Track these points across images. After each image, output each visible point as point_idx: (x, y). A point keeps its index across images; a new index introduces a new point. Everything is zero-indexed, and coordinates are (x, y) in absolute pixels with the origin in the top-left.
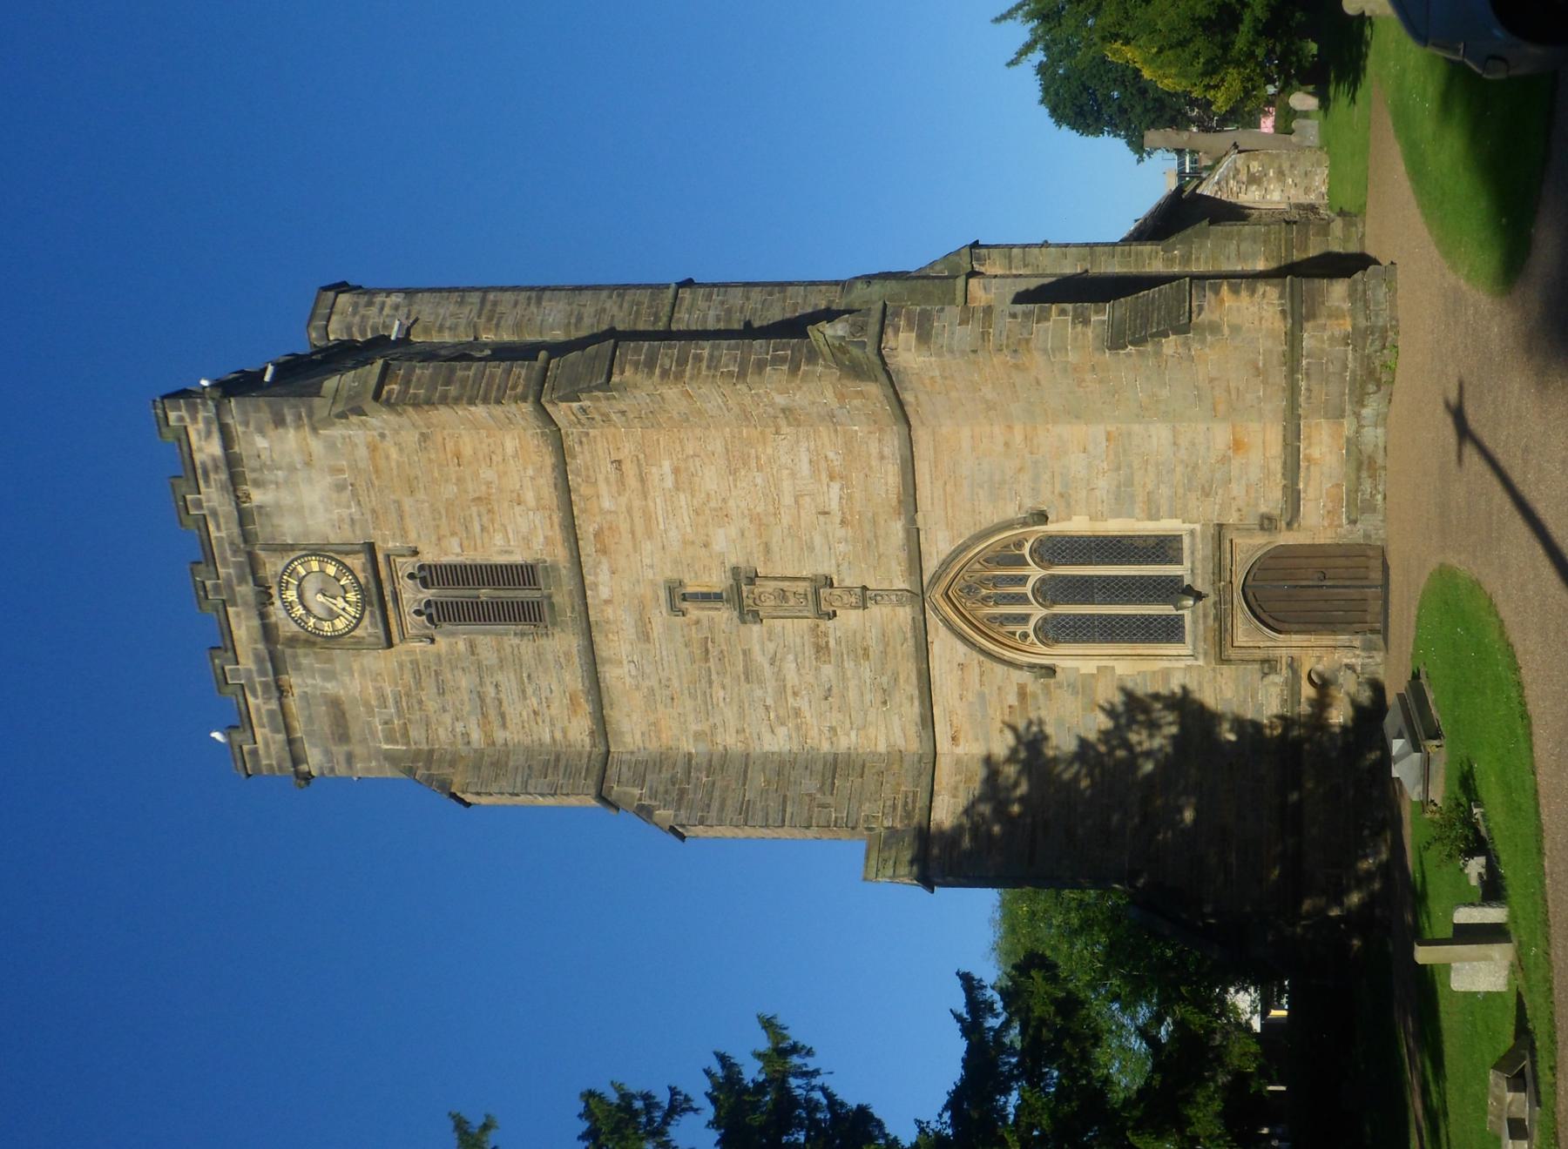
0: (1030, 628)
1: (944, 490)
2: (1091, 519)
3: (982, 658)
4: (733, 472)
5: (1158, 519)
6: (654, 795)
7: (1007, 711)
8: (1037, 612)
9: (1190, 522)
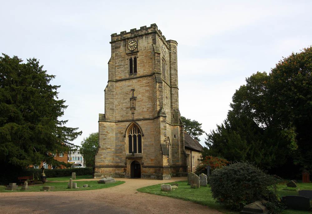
4: (148, 97)
6: (109, 87)
8: (132, 135)
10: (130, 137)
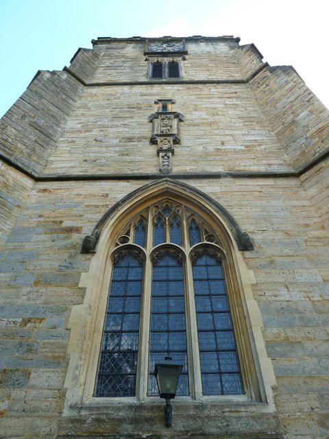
0: (131, 242)
1: (254, 191)
2: (253, 285)
3: (110, 207)
5: (269, 355)
7: (59, 220)
9: (275, 397)
10: (126, 256)
